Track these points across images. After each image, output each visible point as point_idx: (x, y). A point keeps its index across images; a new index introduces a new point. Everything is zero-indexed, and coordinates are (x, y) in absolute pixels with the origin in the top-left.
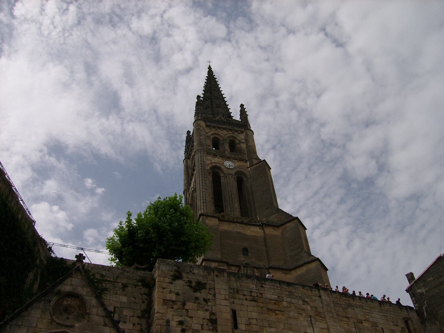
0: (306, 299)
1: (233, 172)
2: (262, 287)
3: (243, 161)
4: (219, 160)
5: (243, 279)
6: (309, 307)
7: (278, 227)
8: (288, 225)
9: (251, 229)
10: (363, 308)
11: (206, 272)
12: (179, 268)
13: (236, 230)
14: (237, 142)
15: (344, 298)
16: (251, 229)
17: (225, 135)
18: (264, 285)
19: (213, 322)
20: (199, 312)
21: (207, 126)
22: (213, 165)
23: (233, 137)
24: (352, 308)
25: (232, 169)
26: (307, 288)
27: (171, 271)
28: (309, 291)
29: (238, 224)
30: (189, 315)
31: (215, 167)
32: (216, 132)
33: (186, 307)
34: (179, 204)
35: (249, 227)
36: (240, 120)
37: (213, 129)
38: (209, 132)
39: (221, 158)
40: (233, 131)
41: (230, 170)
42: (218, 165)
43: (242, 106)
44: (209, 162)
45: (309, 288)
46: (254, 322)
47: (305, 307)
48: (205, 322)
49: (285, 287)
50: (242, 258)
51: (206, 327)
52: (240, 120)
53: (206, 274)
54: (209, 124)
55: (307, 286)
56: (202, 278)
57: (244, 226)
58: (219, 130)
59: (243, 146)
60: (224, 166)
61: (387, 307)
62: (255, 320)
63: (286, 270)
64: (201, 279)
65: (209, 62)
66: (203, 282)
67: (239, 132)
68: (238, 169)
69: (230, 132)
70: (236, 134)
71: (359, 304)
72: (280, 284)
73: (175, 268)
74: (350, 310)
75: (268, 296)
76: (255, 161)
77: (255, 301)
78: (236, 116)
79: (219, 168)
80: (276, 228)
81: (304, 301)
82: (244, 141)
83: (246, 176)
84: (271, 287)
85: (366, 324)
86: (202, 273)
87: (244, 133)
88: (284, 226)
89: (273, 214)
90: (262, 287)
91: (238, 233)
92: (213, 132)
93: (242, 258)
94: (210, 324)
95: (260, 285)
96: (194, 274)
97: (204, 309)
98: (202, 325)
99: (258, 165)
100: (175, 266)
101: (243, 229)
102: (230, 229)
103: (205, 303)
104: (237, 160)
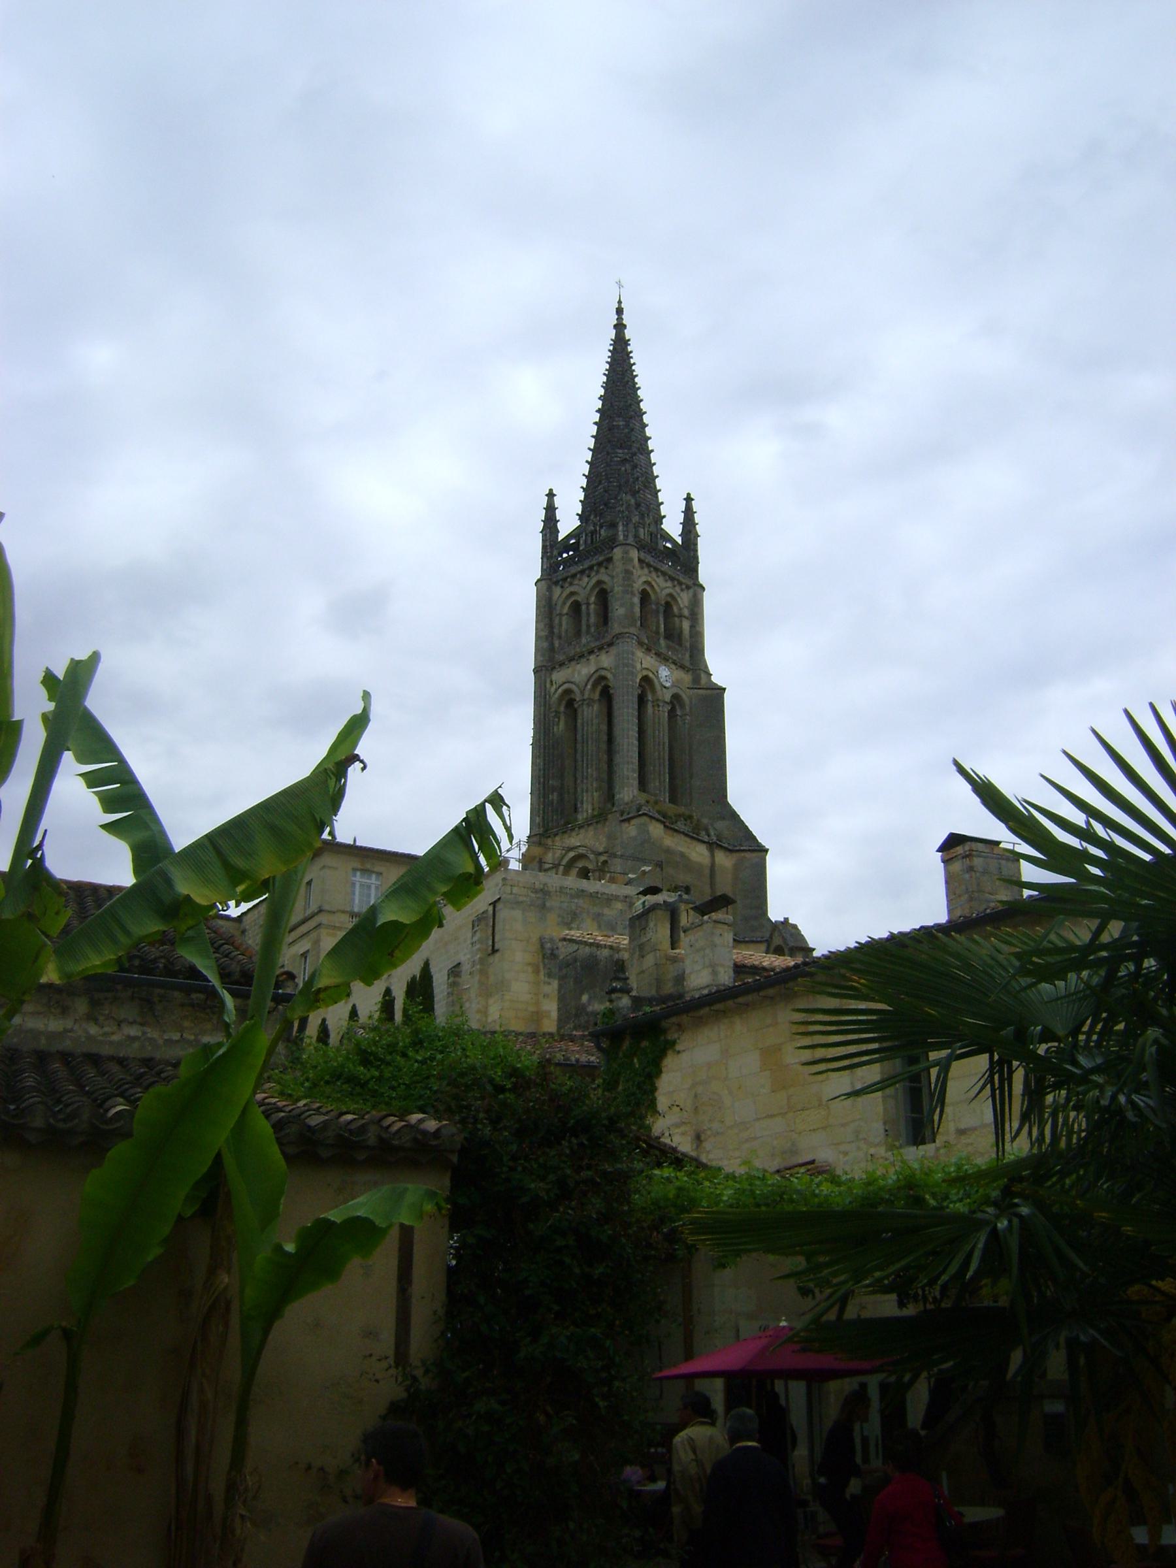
7: (731, 851)
8: (748, 855)
14: (675, 609)
17: (662, 590)
21: (640, 560)
29: (683, 837)
35: (695, 843)
36: (679, 540)
37: (646, 570)
43: (689, 499)
52: (679, 540)
57: (688, 839)
58: (654, 575)
59: (686, 625)
60: (657, 677)
65: (620, 286)
69: (669, 584)
76: (703, 681)
78: (673, 526)
82: (686, 612)
83: (682, 706)
87: (691, 591)
88: (743, 854)
89: (723, 818)
91: (682, 855)
99: (709, 692)
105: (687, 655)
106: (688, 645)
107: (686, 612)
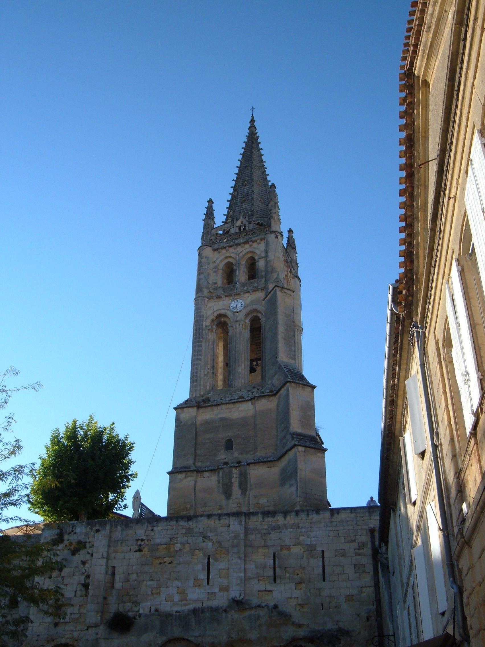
0: (209, 534)
1: (241, 316)
2: (152, 530)
3: (258, 291)
4: (225, 302)
5: (131, 525)
6: (210, 544)
9: (240, 409)
10: (298, 527)
11: (89, 527)
12: (62, 530)
13: (219, 416)
14: (256, 258)
15: (270, 519)
16: (240, 409)
18: (155, 528)
19: (86, 586)
20: (74, 577)
22: (216, 314)
23: (251, 252)
24: (278, 531)
25: (240, 311)
26: (214, 517)
27: (54, 535)
28: (217, 521)
29: (224, 406)
30: (64, 583)
31: (220, 316)
32: (228, 255)
33: (63, 574)
34: (67, 450)
37: (224, 251)
38: (217, 259)
39: (227, 298)
40: (251, 243)
41: (237, 314)
42: (223, 312)
44: (209, 312)
45: (217, 517)
46: (133, 577)
47: (204, 545)
48: (80, 587)
49: (182, 523)
50: (223, 456)
51: (79, 594)
53: (88, 530)
54: (216, 246)
55: (215, 515)
56: (83, 537)
58: (231, 250)
61: (343, 516)
62: (135, 575)
63: (271, 461)
64: (82, 538)
66: (83, 541)
67: (259, 241)
68: (249, 308)
70: (255, 245)
71: (292, 522)
72: (177, 521)
73: (57, 531)
74: (274, 536)
75: (158, 541)
77: (140, 550)
79: (225, 316)
80: (272, 398)
81: (205, 537)
84: (166, 528)
85: (296, 550)
86: (84, 531)
90: (152, 530)
91: (222, 419)
92: (223, 257)
93: (223, 456)
94: (83, 589)
95: (150, 528)
96: (75, 533)
97: (81, 572)
98: (76, 592)
100: (58, 528)
101: (230, 412)
102: (212, 416)
103: (82, 566)
104: (249, 292)
105: (263, 280)
106: (263, 274)
107: (263, 254)
